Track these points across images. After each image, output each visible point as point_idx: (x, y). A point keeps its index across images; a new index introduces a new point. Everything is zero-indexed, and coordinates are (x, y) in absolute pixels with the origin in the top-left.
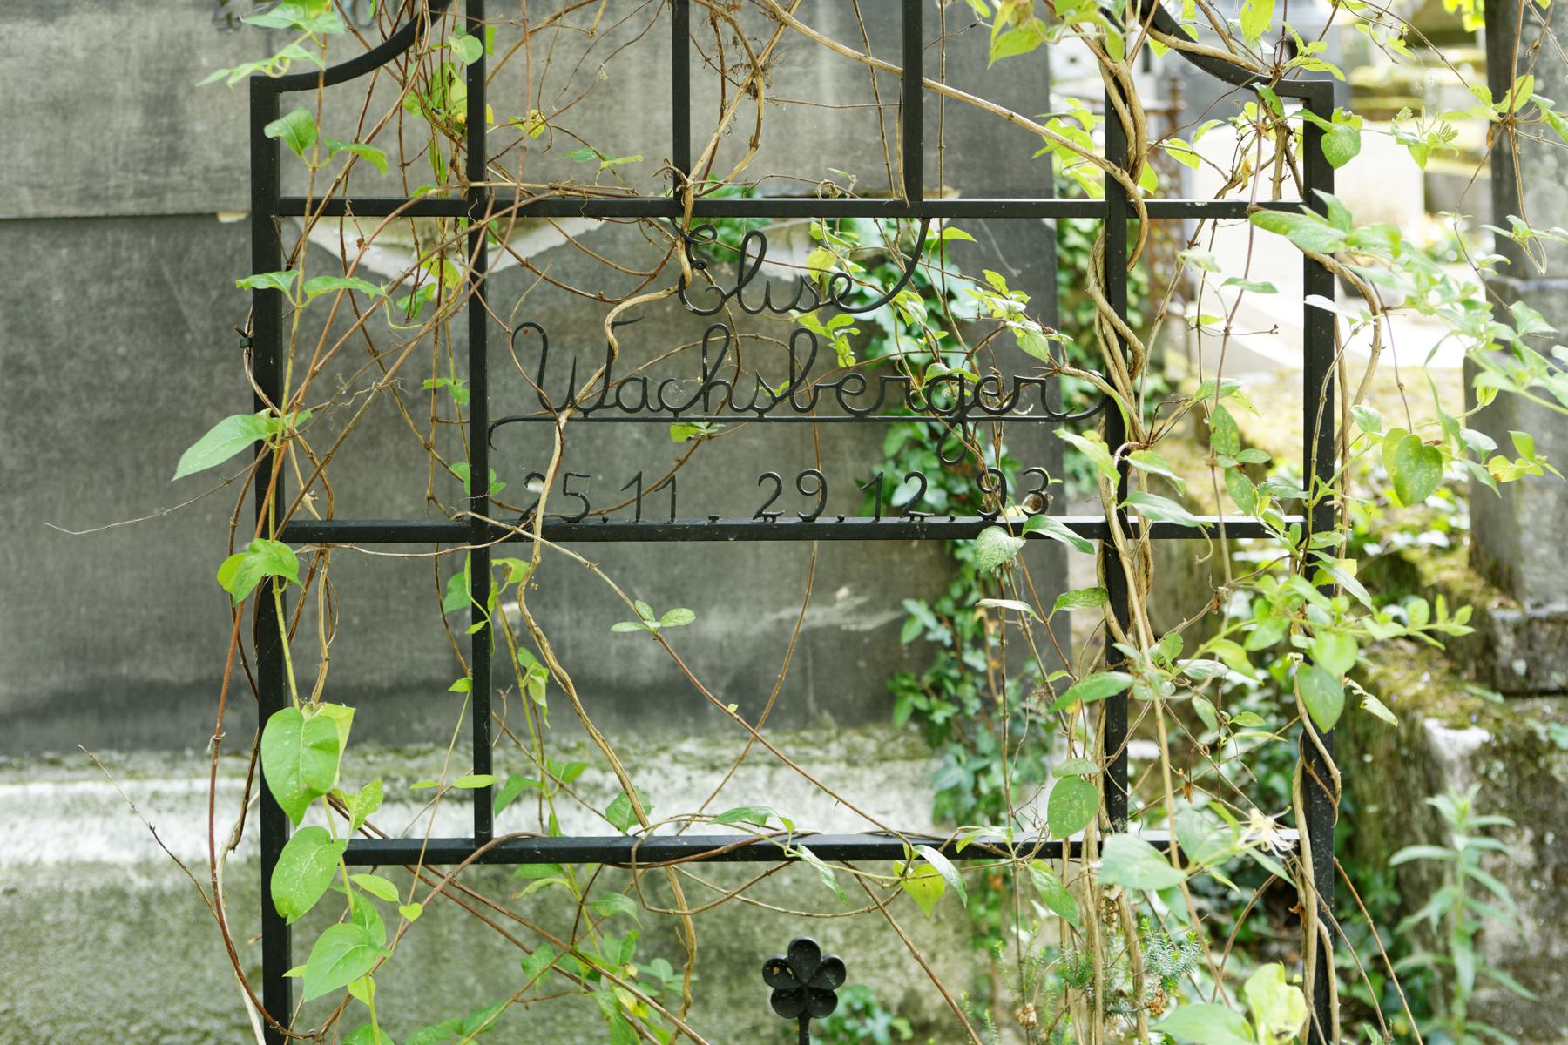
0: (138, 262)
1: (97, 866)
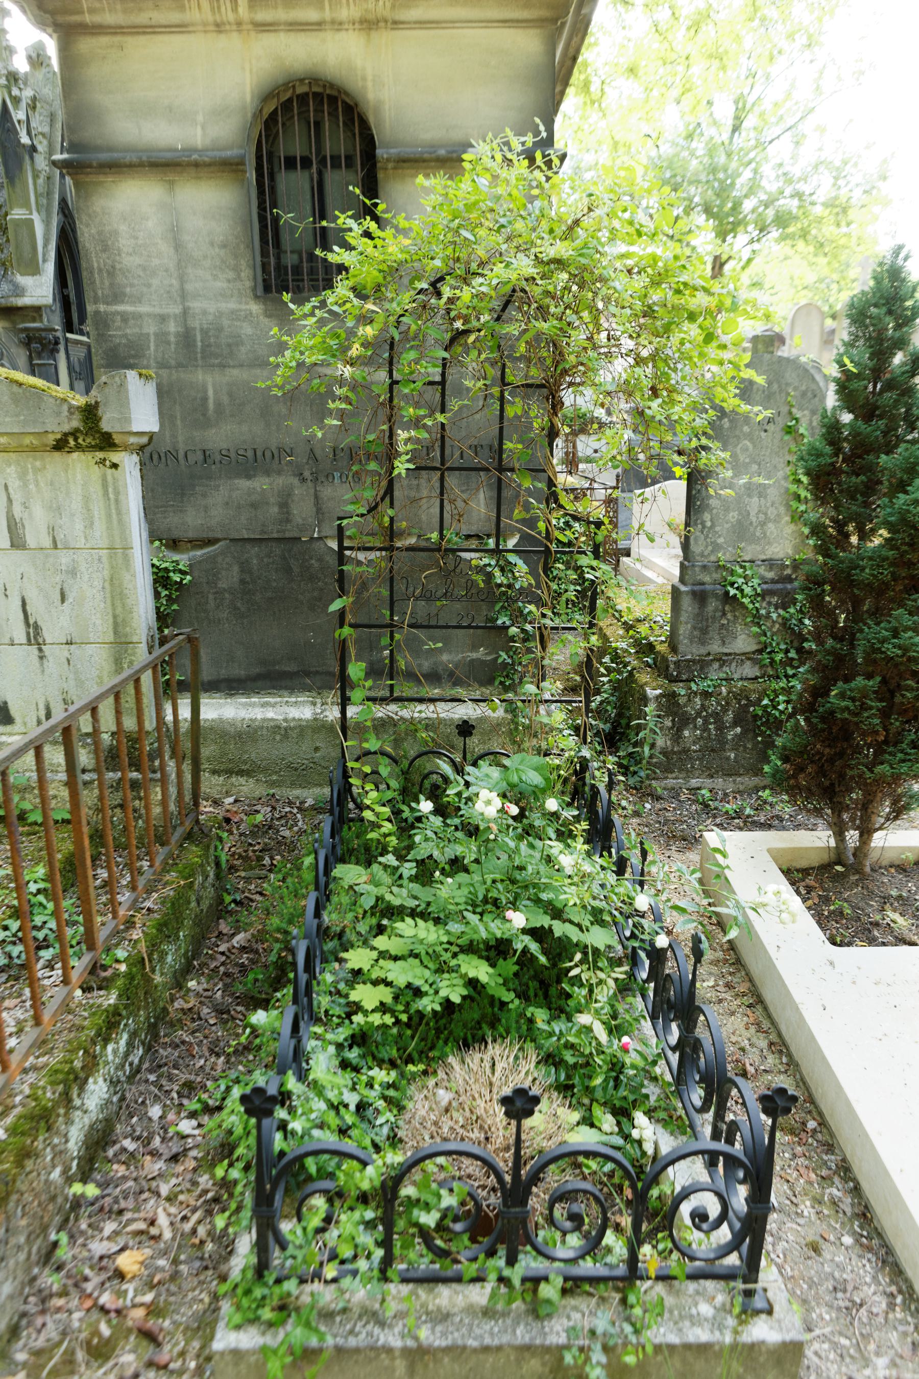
0: (278, 552)
1: (272, 720)
